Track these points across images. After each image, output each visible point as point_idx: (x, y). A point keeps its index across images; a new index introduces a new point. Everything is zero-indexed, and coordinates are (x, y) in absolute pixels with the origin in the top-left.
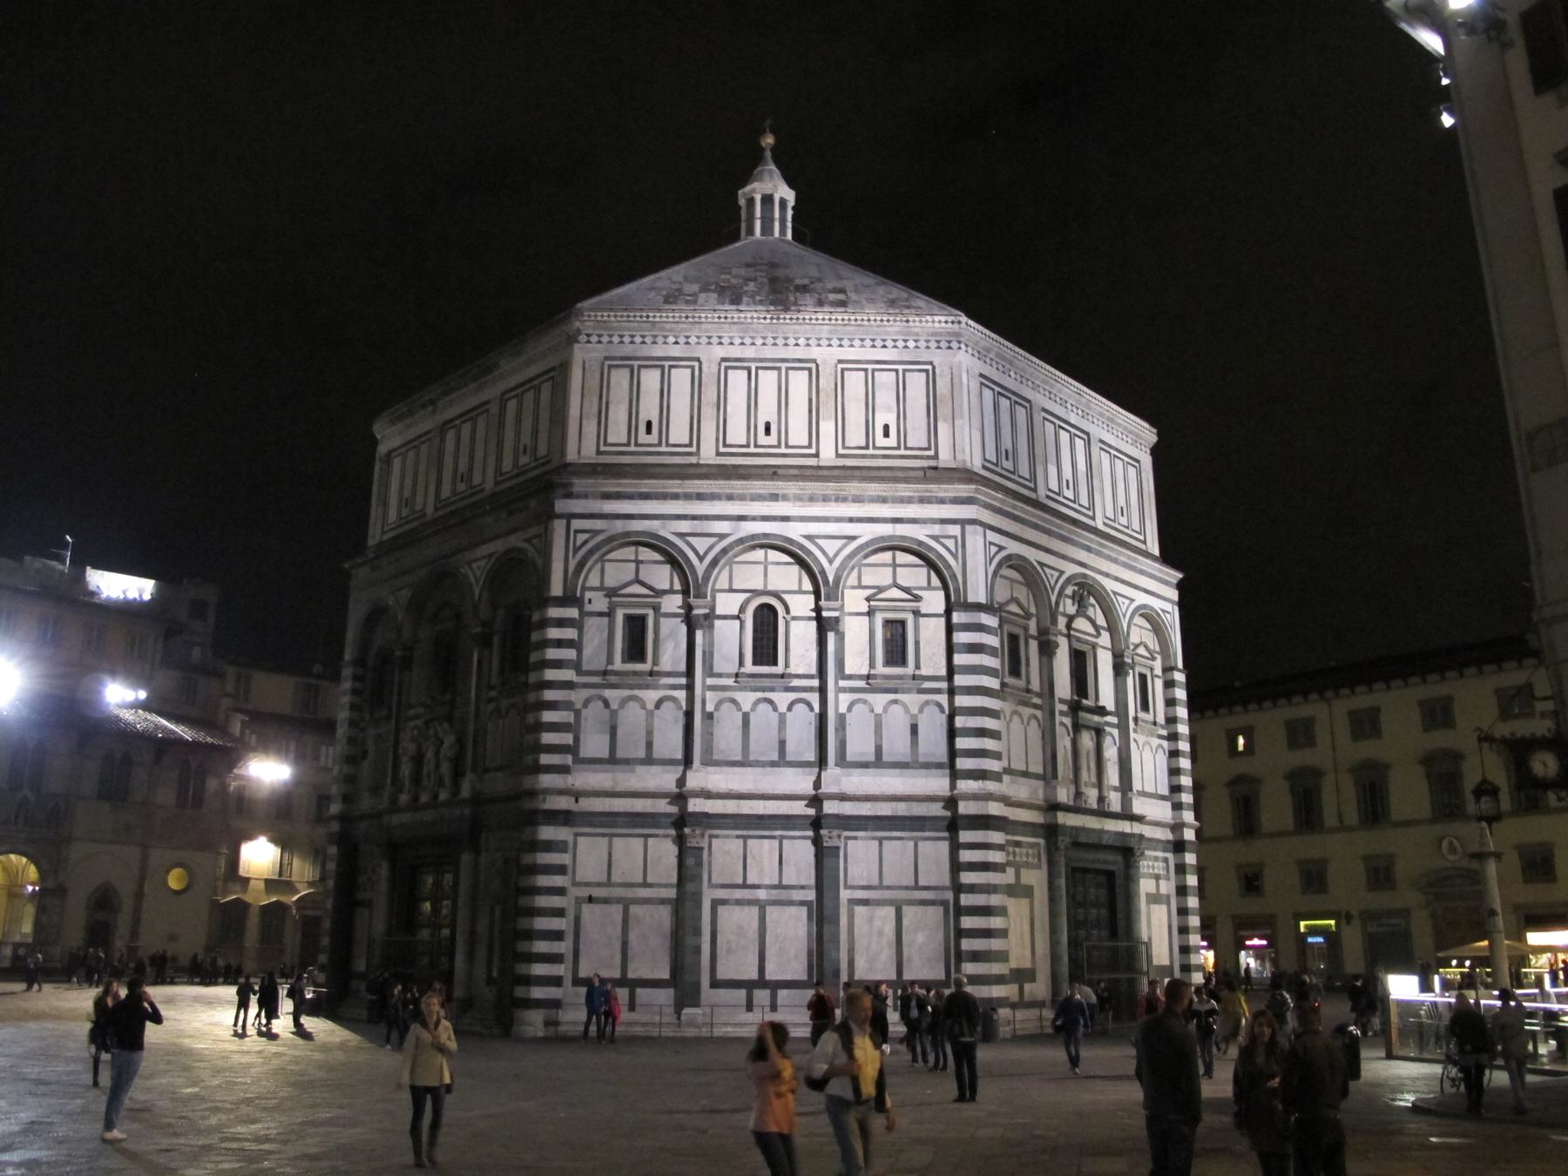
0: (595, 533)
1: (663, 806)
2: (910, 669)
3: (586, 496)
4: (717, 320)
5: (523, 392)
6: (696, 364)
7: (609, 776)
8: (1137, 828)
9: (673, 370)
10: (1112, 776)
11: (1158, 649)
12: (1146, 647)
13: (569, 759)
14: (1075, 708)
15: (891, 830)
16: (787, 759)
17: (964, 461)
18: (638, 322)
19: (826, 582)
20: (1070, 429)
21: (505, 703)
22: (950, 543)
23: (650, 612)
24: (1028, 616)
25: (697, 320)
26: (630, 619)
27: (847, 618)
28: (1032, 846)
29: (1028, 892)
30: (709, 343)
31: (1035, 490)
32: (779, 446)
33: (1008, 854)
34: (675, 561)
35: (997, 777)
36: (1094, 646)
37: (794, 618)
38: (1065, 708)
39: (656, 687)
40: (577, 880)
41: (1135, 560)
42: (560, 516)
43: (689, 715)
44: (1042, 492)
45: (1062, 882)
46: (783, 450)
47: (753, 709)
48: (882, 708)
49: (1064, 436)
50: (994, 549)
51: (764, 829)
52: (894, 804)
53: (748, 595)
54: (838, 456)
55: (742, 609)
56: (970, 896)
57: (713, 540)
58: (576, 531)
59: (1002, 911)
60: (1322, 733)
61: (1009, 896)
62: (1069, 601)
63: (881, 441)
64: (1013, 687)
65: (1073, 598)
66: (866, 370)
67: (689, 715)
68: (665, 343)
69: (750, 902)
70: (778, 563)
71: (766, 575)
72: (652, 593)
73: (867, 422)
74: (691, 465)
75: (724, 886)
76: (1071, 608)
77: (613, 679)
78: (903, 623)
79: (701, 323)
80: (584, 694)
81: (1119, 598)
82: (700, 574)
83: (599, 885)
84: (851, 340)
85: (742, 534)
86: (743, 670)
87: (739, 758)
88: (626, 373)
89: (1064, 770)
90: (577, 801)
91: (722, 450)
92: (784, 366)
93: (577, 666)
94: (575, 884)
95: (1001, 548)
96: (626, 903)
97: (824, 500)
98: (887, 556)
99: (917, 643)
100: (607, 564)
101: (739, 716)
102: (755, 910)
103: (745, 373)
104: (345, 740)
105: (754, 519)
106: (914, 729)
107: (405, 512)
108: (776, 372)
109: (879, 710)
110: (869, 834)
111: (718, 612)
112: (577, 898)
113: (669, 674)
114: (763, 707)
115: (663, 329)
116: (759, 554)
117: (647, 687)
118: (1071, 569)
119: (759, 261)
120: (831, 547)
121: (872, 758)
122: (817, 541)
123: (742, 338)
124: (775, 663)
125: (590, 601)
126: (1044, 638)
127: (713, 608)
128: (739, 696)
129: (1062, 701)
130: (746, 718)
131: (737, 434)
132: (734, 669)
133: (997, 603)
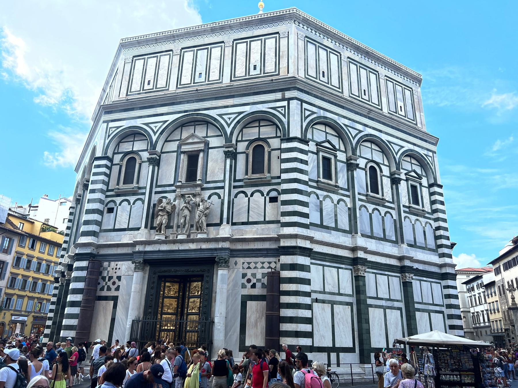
0: (313, 113)
22: (430, 159)
26: (324, 158)
39: (337, 194)
53: (367, 161)
58: (305, 109)
73: (395, 103)
83: (320, 292)
92: (368, 69)
96: (333, 303)
105: (370, 127)
106: (424, 232)
107: (146, 87)
114: (376, 212)
117: (334, 192)
122: (392, 144)
124: (378, 193)
128: (368, 205)
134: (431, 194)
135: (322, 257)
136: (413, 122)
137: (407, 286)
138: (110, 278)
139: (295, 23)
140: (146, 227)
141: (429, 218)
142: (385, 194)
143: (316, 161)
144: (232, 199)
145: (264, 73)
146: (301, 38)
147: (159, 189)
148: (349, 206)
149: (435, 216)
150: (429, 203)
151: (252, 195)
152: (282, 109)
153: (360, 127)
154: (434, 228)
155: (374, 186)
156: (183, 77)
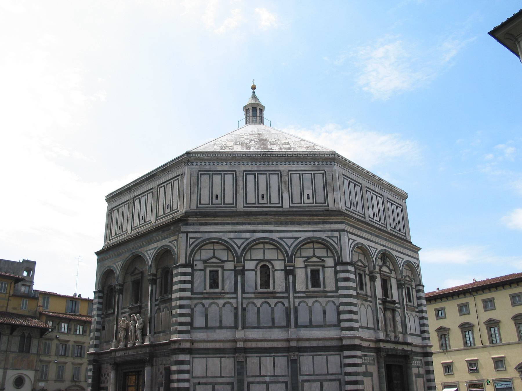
1: (228, 345)
2: (322, 288)
3: (193, 224)
4: (242, 156)
5: (167, 185)
6: (234, 173)
7: (205, 334)
8: (410, 348)
9: (225, 175)
10: (399, 328)
11: (413, 278)
12: (409, 277)
13: (188, 328)
14: (384, 302)
15: (317, 352)
16: (275, 325)
17: (339, 207)
18: (211, 157)
19: (288, 256)
20: (377, 194)
21: (162, 306)
22: (335, 239)
23: (220, 270)
24: (365, 266)
25: (234, 156)
26: (211, 271)
27: (296, 269)
28: (371, 356)
29: (370, 374)
30: (239, 165)
31: (365, 218)
32: (267, 203)
33: (363, 360)
34: (228, 248)
35: (357, 329)
36: (390, 277)
37: (276, 270)
38: (380, 302)
39: (223, 298)
40: (194, 376)
41: (403, 243)
42: (183, 232)
43: (236, 309)
44: (367, 219)
45: (383, 370)
46: (269, 205)
47: (261, 306)
48: (311, 304)
49: (374, 197)
50: (351, 241)
51: (268, 353)
52: (318, 342)
53: (257, 261)
54: (290, 206)
55: (256, 267)
56: (349, 377)
57: (244, 240)
58: (190, 238)
59: (362, 382)
60: (472, 307)
61: (364, 376)
62: (380, 260)
63: (306, 201)
64: (361, 294)
65: (381, 259)
66: (299, 174)
67: (236, 309)
68: (222, 165)
69: (263, 383)
70: (269, 249)
71: (264, 254)
72: (220, 262)
73: (301, 193)
74: (234, 212)
75: (252, 376)
76: (381, 263)
77: (206, 296)
78: (318, 271)
79: (236, 157)
80: (195, 301)
81: (398, 258)
82: (239, 254)
83: (203, 377)
84: (293, 162)
85: (255, 238)
86: (257, 291)
87: (256, 325)
88: (207, 176)
89: (381, 326)
90: (193, 344)
91: (245, 205)
92: (268, 173)
93: (192, 291)
94: (193, 377)
95: (354, 240)
96: (214, 385)
97: (286, 224)
98: (311, 245)
99: (324, 278)
100: (202, 251)
101: (256, 308)
102: (265, 386)
103: (253, 176)
104: (95, 323)
105: (259, 232)
106: (324, 312)
108: (265, 175)
109: (310, 305)
110: (309, 354)
111: (246, 268)
112: (194, 383)
113: (228, 293)
114: (265, 305)
115: (221, 160)
116: (261, 246)
117: (219, 298)
118: (380, 248)
119: (254, 133)
120: (289, 242)
121: (308, 324)
123: (252, 162)
124: (269, 287)
125: (196, 265)
126: (372, 275)
127: (244, 267)
128: (255, 301)
129: (379, 299)
130: (258, 309)
131: (251, 199)
132: (252, 290)
133: (354, 262)
134: (336, 273)
135: (205, 351)
136: (324, 205)
137: (294, 364)
138: (105, 374)
139: (189, 165)
140: (116, 339)
141: (333, 297)
142: (276, 287)
143: (203, 278)
144: (153, 315)
145: (172, 211)
146: (194, 175)
147: (123, 311)
148: (235, 306)
149: (341, 292)
150: (334, 281)
151: (163, 311)
152: (175, 242)
153: (247, 235)
154: (337, 304)
155: (266, 281)
156: (134, 221)
